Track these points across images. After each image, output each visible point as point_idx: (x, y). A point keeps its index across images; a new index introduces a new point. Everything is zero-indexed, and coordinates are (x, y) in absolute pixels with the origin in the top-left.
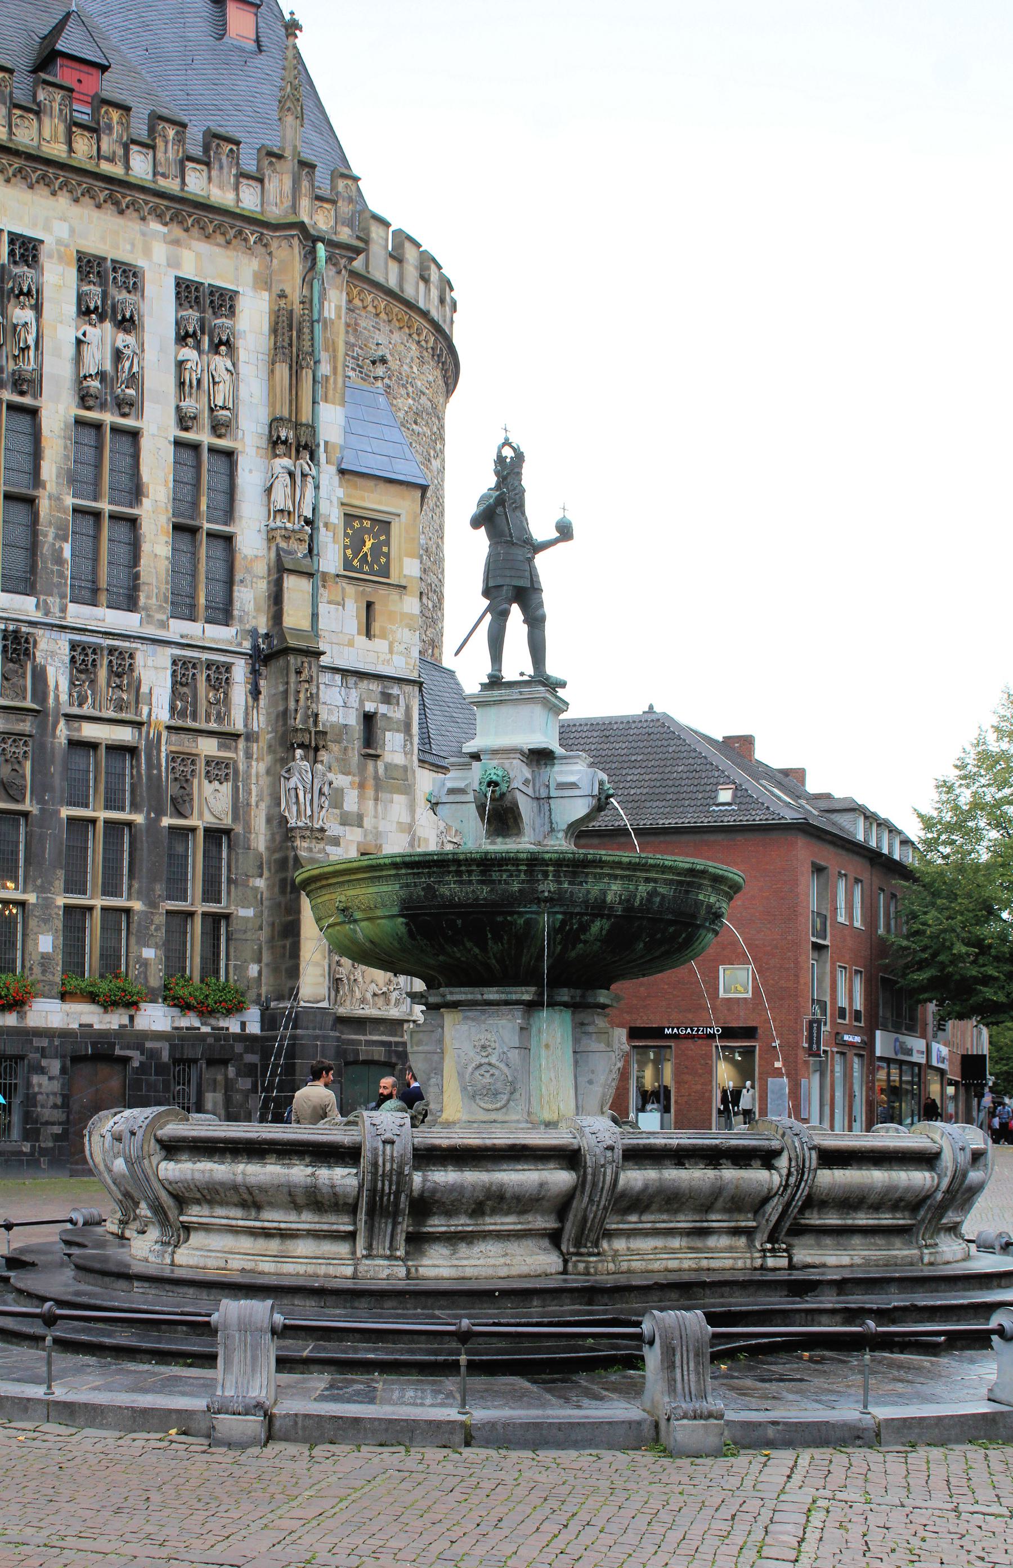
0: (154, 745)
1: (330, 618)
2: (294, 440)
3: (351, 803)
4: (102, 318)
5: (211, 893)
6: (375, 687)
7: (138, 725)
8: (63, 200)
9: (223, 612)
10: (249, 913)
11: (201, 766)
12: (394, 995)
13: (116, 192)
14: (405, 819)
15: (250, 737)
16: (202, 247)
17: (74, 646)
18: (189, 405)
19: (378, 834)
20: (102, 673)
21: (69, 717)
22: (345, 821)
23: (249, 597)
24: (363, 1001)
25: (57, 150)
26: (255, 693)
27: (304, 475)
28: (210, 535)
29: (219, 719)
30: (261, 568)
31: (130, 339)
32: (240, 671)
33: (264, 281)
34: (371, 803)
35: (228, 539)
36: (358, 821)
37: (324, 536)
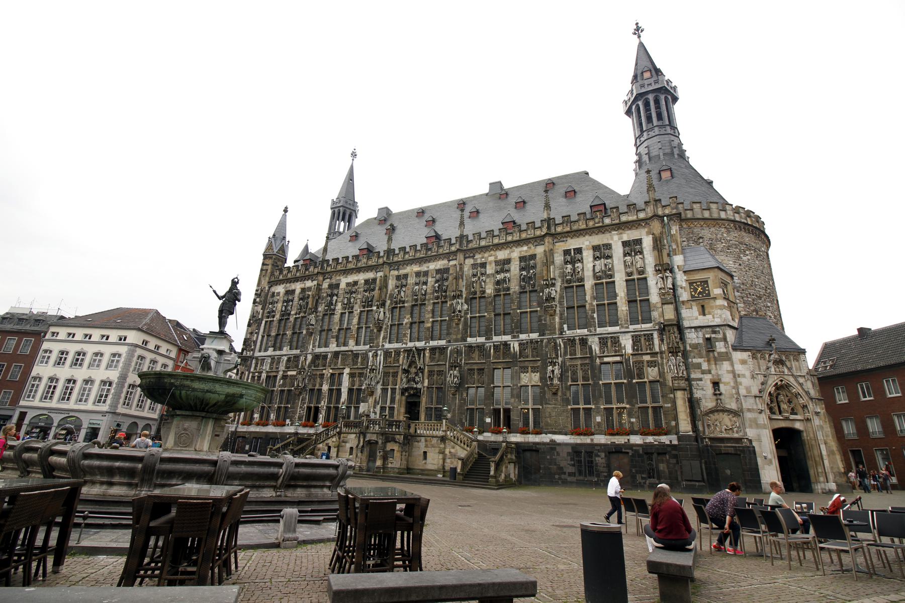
0: (628, 360)
1: (685, 313)
2: (664, 268)
3: (705, 366)
4: (600, 259)
5: (655, 399)
6: (708, 330)
7: (622, 355)
8: (587, 237)
9: (649, 320)
10: (669, 405)
11: (645, 364)
12: (735, 429)
13: (602, 229)
14: (730, 368)
15: (662, 353)
16: (629, 232)
17: (600, 338)
18: (629, 270)
19: (718, 375)
20: (609, 344)
21: (599, 357)
22: (703, 372)
23: (655, 314)
24: (722, 432)
25: (584, 227)
26: (662, 340)
27: (667, 277)
28: (640, 301)
29: (650, 349)
30: (659, 305)
31: (609, 261)
32: (656, 335)
33: (648, 233)
34: (713, 366)
35: (648, 300)
36: (709, 372)
37: (680, 291)
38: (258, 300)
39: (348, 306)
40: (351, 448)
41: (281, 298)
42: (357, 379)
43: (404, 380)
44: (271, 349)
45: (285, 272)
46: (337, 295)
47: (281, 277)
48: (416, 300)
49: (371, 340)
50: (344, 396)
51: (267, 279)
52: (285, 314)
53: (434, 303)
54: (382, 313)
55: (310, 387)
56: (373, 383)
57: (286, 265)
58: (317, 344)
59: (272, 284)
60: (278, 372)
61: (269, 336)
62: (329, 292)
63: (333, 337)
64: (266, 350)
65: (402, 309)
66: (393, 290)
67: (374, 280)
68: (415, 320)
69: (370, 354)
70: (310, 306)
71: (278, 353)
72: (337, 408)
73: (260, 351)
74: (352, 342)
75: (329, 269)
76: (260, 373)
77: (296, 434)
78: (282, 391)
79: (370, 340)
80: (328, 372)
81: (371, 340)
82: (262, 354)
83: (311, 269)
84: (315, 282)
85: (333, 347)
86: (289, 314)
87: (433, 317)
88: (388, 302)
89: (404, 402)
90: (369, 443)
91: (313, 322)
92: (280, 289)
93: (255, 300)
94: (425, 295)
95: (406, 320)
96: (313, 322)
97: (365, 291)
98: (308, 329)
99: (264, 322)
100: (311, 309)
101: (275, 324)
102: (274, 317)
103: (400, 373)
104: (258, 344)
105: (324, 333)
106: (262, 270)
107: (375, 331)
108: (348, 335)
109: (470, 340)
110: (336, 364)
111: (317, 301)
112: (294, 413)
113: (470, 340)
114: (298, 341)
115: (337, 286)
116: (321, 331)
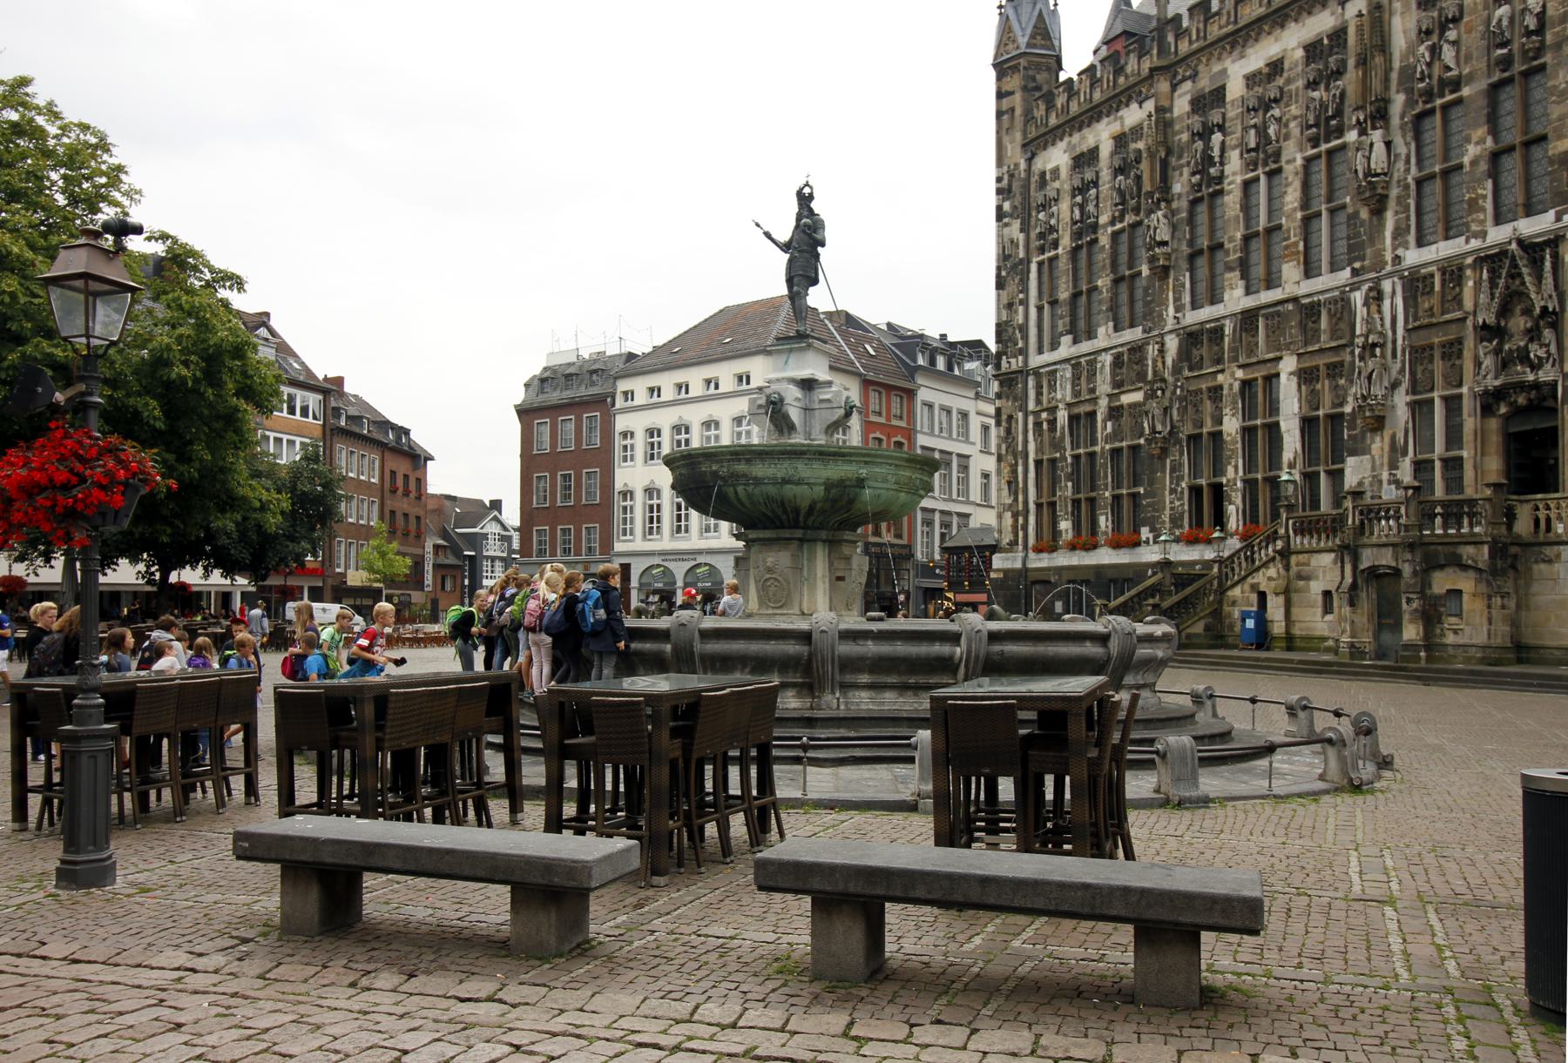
38: (1007, 206)
39: (1264, 155)
40: (1327, 594)
41: (1064, 183)
42: (1324, 386)
43: (1488, 362)
44: (1066, 340)
45: (1060, 101)
46: (1221, 128)
47: (1053, 121)
48: (1506, 63)
49: (1355, 251)
50: (1291, 443)
51: (1018, 136)
52: (1085, 228)
54: (1379, 148)
55: (1187, 429)
56: (1378, 391)
57: (1063, 77)
58: (1187, 298)
59: (1033, 147)
60: (1094, 400)
61: (1054, 303)
62: (1196, 122)
63: (1230, 269)
64: (1055, 345)
65: (1455, 113)
66: (1411, 50)
67: (1339, 35)
69: (1358, 297)
70: (1147, 187)
71: (1086, 347)
72: (1273, 482)
73: (1040, 352)
74: (1290, 272)
75: (1184, 47)
76: (1053, 410)
77: (1166, 564)
78: (1116, 452)
79: (1351, 248)
80: (1231, 378)
81: (1355, 251)
82: (1048, 357)
83: (1132, 65)
84: (1150, 106)
85: (1236, 299)
86: (1095, 227)
88: (1398, 100)
89: (1495, 439)
90: (1373, 574)
91: (1163, 234)
92: (1057, 157)
93: (999, 208)
94: (1540, 30)
95: (1474, 150)
96: (1163, 234)
97: (1312, 85)
98: (1152, 260)
99: (1034, 267)
100: (1150, 194)
101: (1064, 264)
102: (1055, 245)
103: (1469, 343)
104: (1033, 331)
105: (1202, 262)
106: (999, 114)
107: (1364, 214)
108: (1277, 250)
110: (1251, 350)
111: (1165, 164)
112: (1158, 507)
114: (1132, 301)
115: (1219, 95)
116: (1192, 257)
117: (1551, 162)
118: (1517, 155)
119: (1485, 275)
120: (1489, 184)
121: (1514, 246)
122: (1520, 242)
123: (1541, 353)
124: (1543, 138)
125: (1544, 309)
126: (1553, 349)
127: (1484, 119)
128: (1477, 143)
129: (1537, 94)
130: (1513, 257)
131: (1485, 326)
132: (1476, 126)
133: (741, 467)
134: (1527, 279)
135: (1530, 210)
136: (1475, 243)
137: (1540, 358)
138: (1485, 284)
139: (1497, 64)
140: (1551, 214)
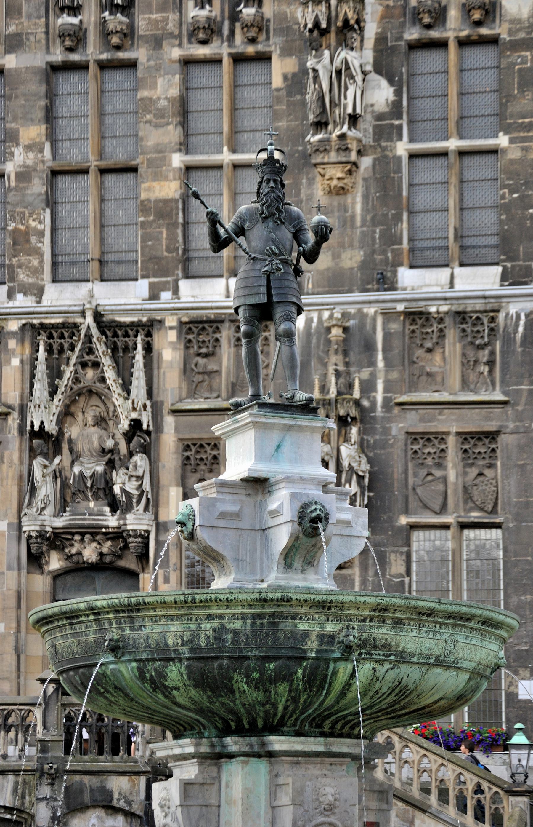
43: (46, 489)
48: (76, 38)
53: (187, 62)
68: (74, 154)
87: (185, 147)
109: (415, 282)
113: (415, 282)
117: (144, 207)
118: (92, 178)
119: (42, 354)
120: (48, 211)
121: (89, 319)
122: (98, 316)
123: (131, 487)
124: (134, 170)
125: (136, 424)
126: (147, 486)
127: (40, 114)
128: (28, 148)
129: (117, 102)
130: (89, 337)
131: (41, 434)
132: (28, 120)
133: (383, 633)
134: (110, 374)
135: (106, 270)
136: (22, 302)
137: (128, 495)
138: (41, 368)
139: (62, 36)
140: (142, 287)
